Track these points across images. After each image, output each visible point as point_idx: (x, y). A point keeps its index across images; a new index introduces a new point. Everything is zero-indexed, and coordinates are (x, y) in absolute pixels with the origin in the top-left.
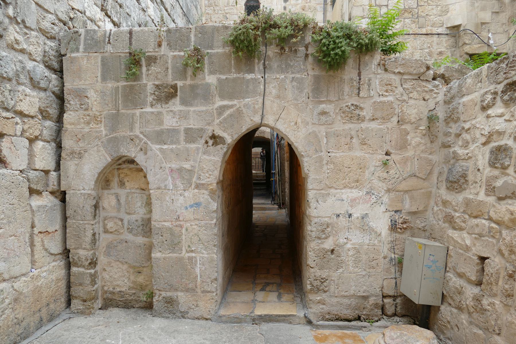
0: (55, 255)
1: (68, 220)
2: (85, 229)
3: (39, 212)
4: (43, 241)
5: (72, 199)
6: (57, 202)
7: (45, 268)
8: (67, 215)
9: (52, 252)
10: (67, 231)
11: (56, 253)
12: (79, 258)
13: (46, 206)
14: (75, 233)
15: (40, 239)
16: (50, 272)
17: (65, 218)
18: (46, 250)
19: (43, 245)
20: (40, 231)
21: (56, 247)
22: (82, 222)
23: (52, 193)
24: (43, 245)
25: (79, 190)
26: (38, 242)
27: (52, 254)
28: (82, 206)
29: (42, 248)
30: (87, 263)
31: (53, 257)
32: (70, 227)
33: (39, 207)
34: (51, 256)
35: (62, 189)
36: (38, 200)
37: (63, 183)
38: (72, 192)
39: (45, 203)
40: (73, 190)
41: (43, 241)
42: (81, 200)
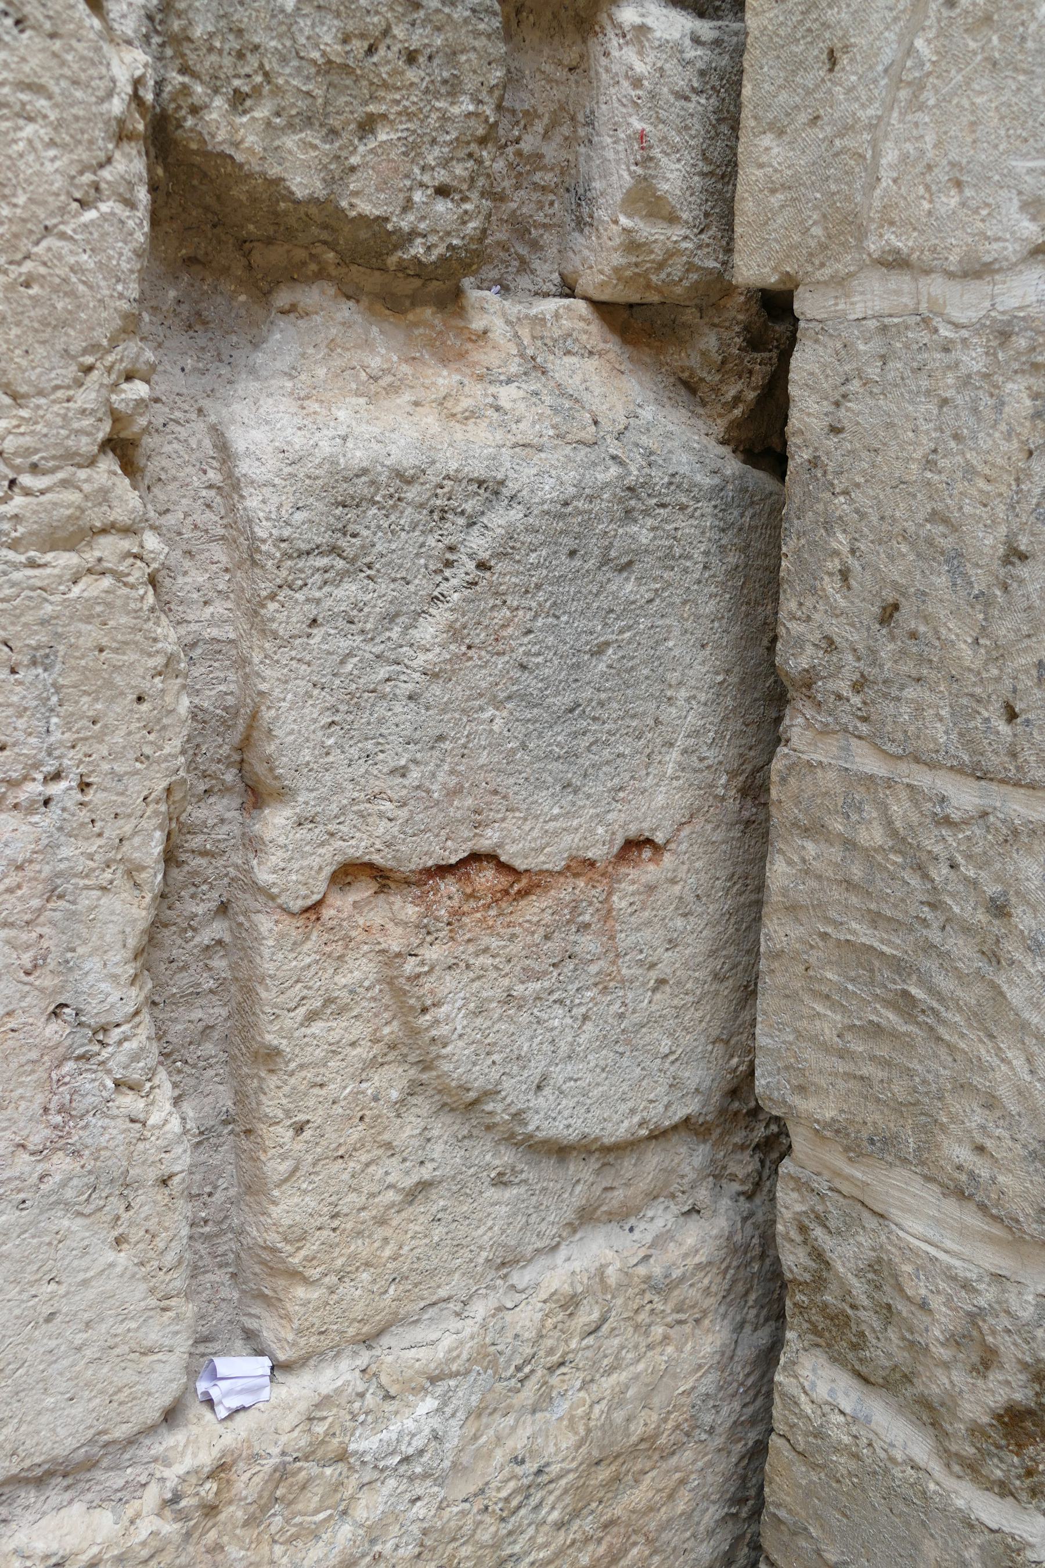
0: (608, 1153)
1: (798, 726)
2: (999, 909)
3: (359, 566)
4: (403, 994)
5: (859, 411)
6: (685, 446)
7: (440, 1340)
8: (795, 661)
9: (557, 1118)
10: (779, 872)
11: (621, 1129)
12: (879, 1271)
13: (491, 489)
14: (864, 934)
15: (360, 970)
16: (507, 1375)
17: (765, 696)
18: (467, 1106)
19: (415, 1048)
20: (359, 846)
21: (612, 1057)
22: (964, 797)
23: (636, 322)
24: (415, 1048)
25: (977, 271)
26: (332, 1006)
27: (560, 1151)
28: (989, 543)
29: (391, 1081)
30: (982, 1399)
31: (581, 1182)
32: (814, 830)
33: (355, 496)
34: (542, 1174)
35: (753, 269)
36: (379, 388)
37: (764, 156)
38: (875, 296)
39: (473, 447)
40: (896, 262)
41: (403, 994)
42: (995, 446)
